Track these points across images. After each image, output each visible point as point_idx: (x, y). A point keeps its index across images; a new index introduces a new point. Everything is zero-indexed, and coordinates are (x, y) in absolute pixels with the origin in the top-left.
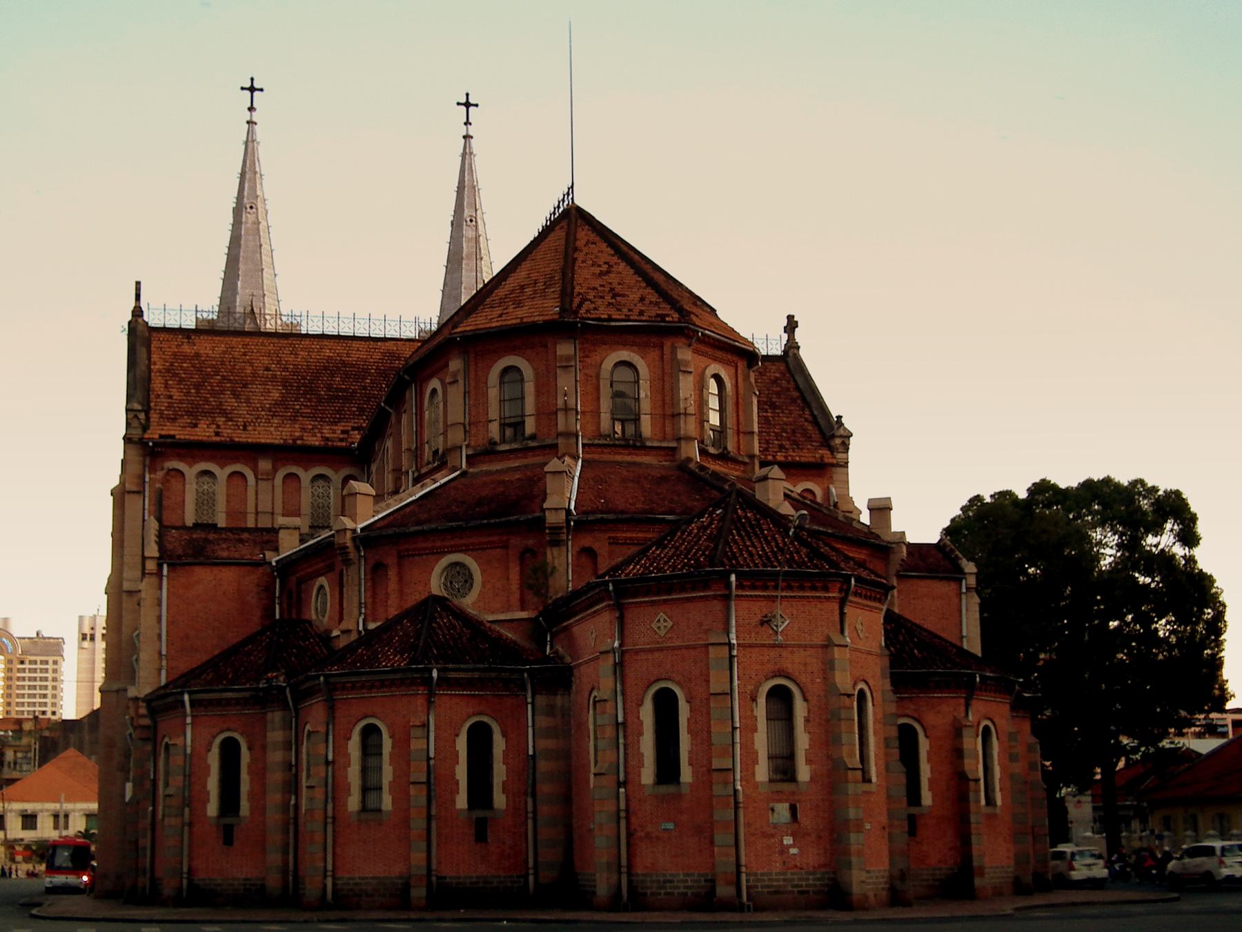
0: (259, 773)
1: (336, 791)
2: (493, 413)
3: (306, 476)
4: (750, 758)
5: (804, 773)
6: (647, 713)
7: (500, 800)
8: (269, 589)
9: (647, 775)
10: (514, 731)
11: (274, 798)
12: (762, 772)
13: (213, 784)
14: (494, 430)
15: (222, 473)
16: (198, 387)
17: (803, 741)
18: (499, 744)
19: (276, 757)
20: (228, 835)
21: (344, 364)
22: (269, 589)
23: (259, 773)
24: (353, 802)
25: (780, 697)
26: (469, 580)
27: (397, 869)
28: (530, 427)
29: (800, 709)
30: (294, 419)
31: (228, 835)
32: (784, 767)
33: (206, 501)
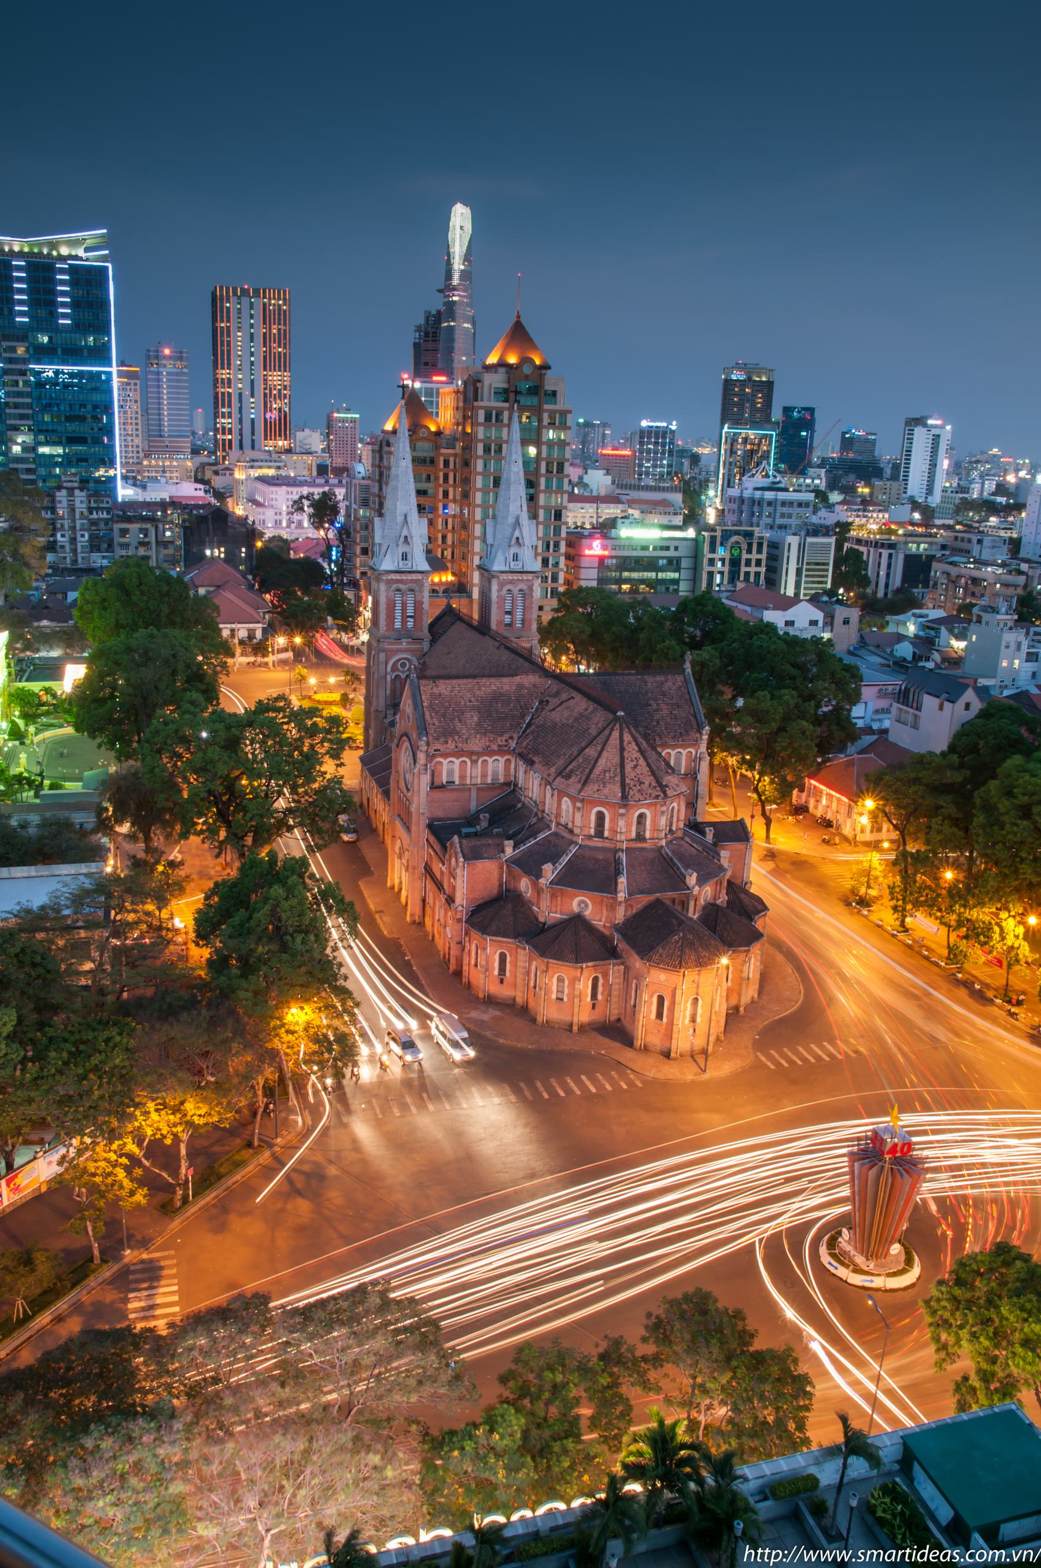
0: (515, 965)
1: (548, 992)
2: (593, 825)
3: (490, 760)
4: (684, 1017)
5: (699, 1020)
6: (655, 1000)
7: (600, 997)
8: (501, 868)
9: (653, 1016)
10: (606, 976)
11: (520, 976)
12: (687, 1021)
13: (497, 965)
14: (592, 832)
15: (457, 762)
16: (444, 716)
17: (699, 1011)
18: (601, 981)
19: (520, 964)
20: (502, 981)
21: (502, 695)
22: (501, 868)
23: (515, 965)
24: (554, 996)
25: (696, 1000)
26: (587, 905)
27: (568, 1018)
28: (606, 834)
29: (700, 1002)
30: (485, 734)
31: (502, 981)
32: (693, 1020)
33: (450, 772)
